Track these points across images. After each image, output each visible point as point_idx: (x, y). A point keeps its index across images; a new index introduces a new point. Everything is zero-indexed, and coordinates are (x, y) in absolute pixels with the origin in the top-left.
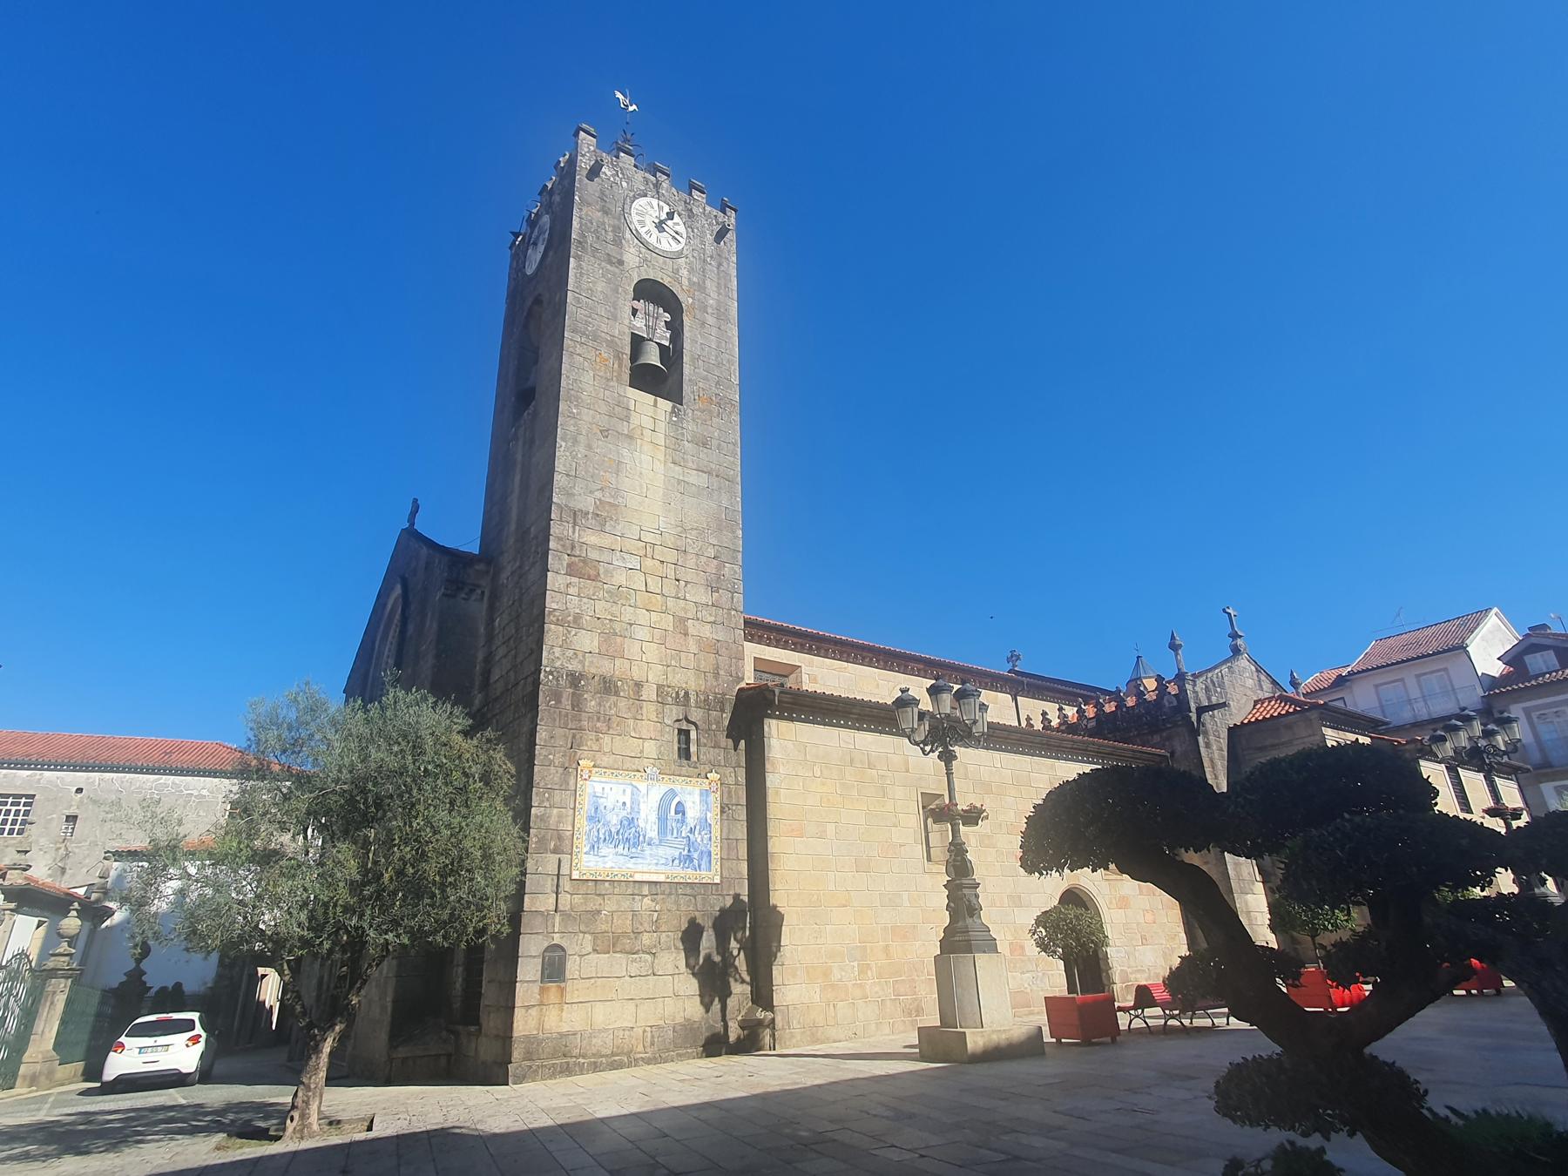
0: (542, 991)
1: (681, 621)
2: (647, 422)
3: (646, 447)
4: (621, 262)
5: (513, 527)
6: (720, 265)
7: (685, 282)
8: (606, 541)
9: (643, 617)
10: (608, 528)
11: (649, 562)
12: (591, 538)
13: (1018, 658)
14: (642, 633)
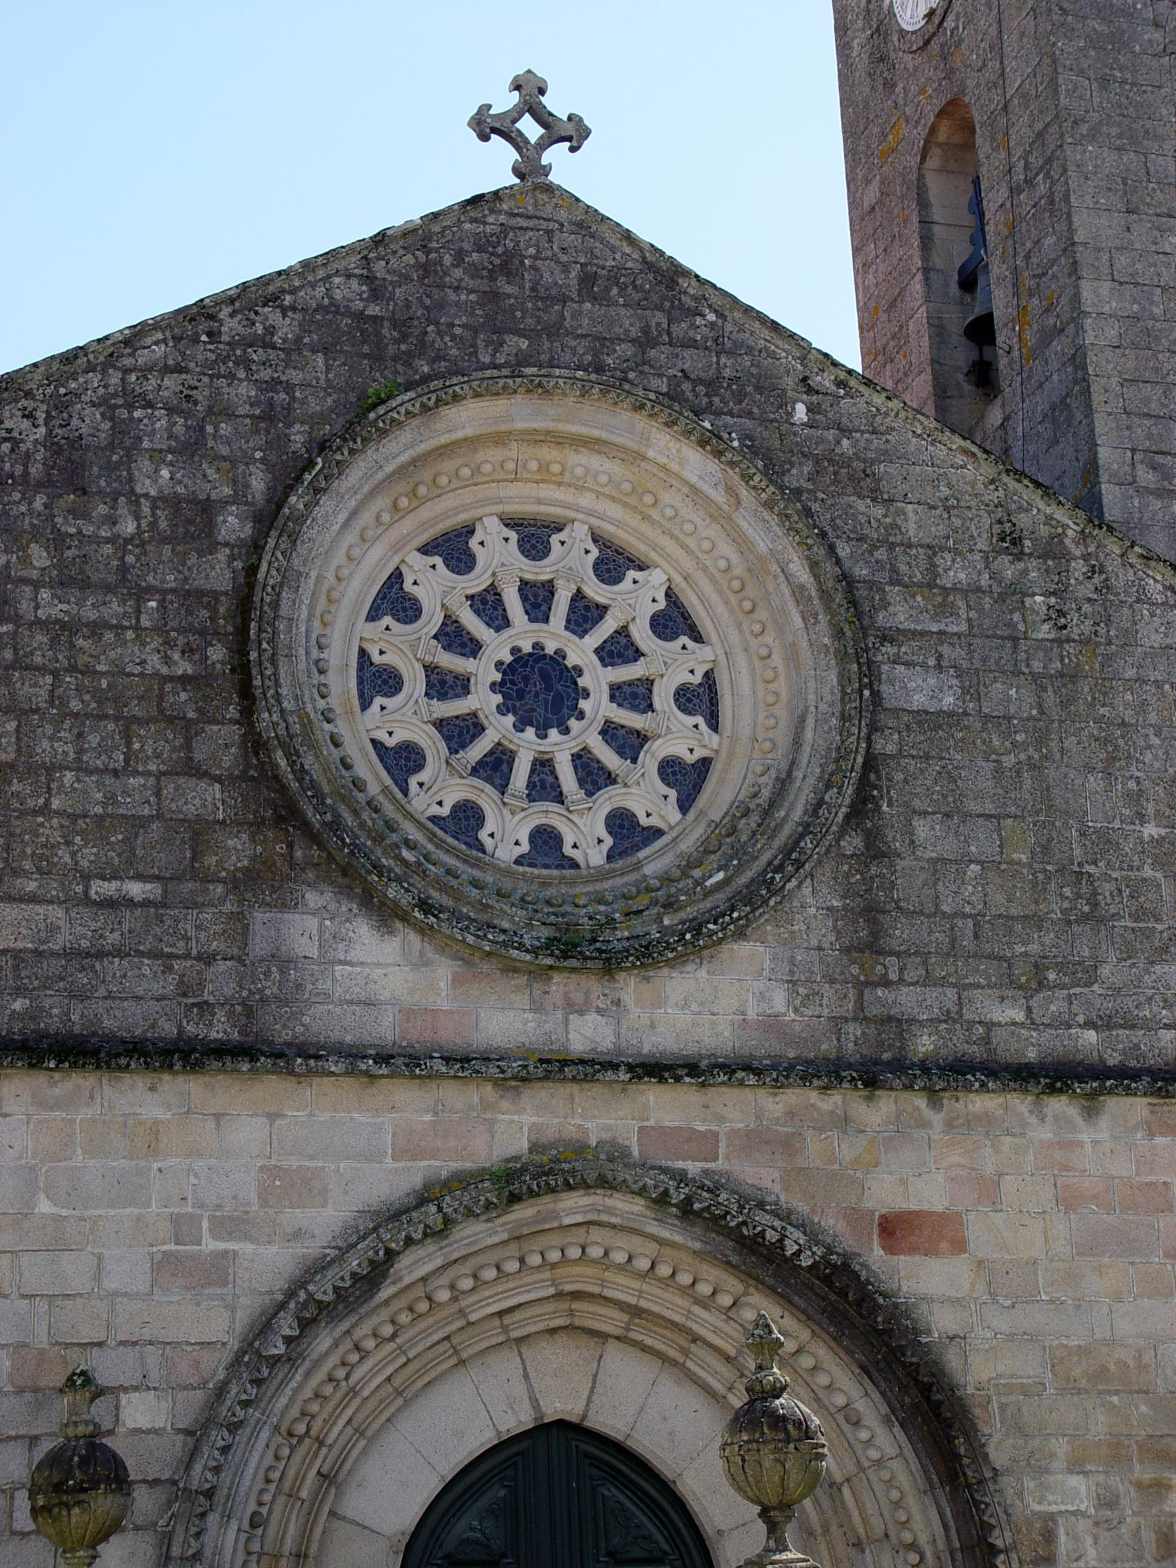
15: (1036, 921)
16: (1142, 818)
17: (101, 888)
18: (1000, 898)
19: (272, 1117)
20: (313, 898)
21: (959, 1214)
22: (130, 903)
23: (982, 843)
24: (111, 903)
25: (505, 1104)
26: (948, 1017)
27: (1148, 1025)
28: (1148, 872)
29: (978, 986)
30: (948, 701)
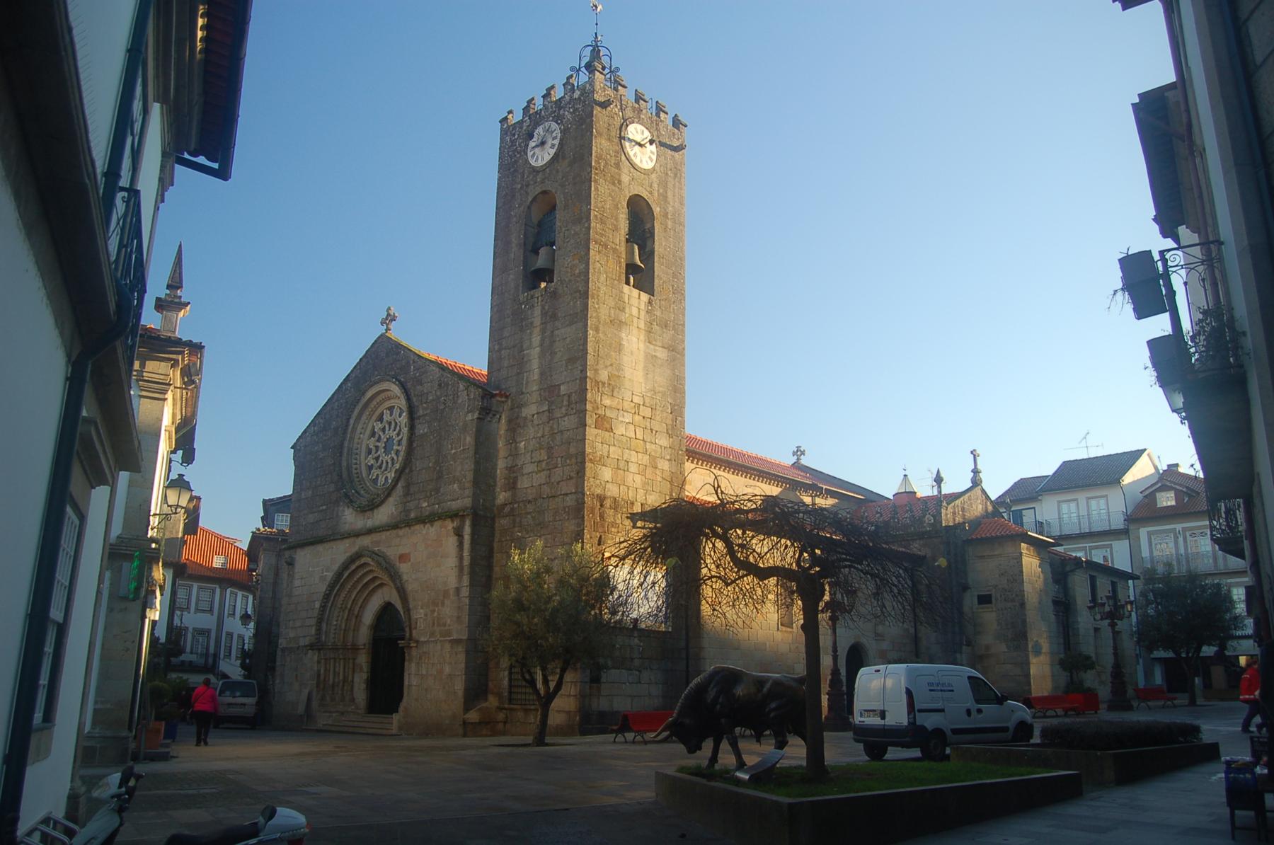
0: (591, 688)
1: (653, 459)
2: (635, 311)
3: (635, 331)
4: (620, 182)
5: (535, 376)
6: (676, 175)
7: (656, 194)
8: (615, 403)
9: (634, 457)
10: (615, 394)
11: (637, 417)
12: (607, 402)
13: (803, 453)
14: (633, 468)
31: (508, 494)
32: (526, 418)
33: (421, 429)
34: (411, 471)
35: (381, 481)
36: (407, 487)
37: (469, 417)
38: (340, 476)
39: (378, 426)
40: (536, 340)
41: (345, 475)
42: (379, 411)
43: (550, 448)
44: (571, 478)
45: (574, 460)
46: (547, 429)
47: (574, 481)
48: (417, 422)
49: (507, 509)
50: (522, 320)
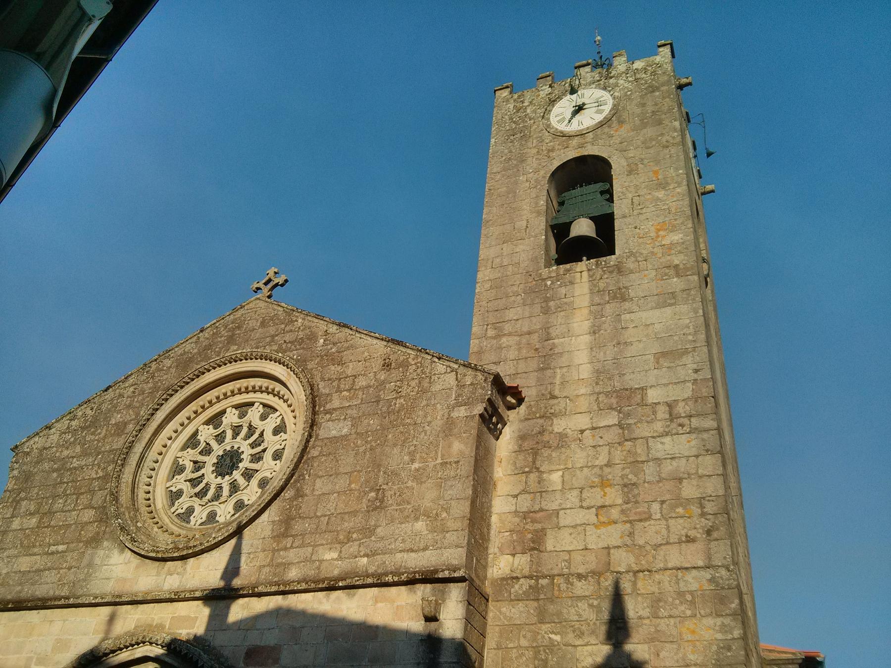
15: (354, 513)
16: (413, 461)
17: (53, 548)
18: (342, 506)
19: (64, 621)
20: (106, 544)
21: (280, 646)
22: (58, 552)
23: (342, 483)
24: (53, 553)
25: (132, 611)
26: (306, 560)
27: (391, 552)
28: (410, 484)
29: (322, 545)
30: (345, 431)
31: (522, 562)
32: (562, 436)
33: (330, 429)
34: (299, 494)
35: (200, 515)
36: (287, 521)
37: (461, 412)
38: (115, 497)
39: (207, 434)
40: (581, 322)
41: (124, 497)
42: (217, 408)
43: (628, 487)
44: (690, 540)
45: (695, 510)
46: (618, 455)
47: (699, 546)
48: (322, 418)
49: (525, 584)
50: (547, 300)
